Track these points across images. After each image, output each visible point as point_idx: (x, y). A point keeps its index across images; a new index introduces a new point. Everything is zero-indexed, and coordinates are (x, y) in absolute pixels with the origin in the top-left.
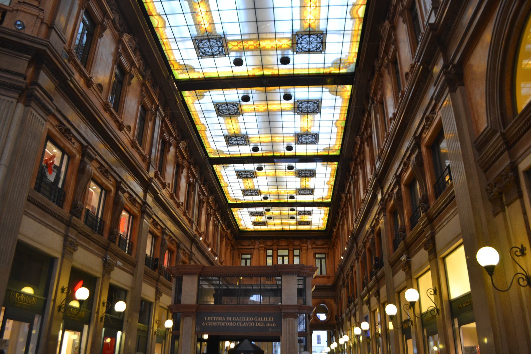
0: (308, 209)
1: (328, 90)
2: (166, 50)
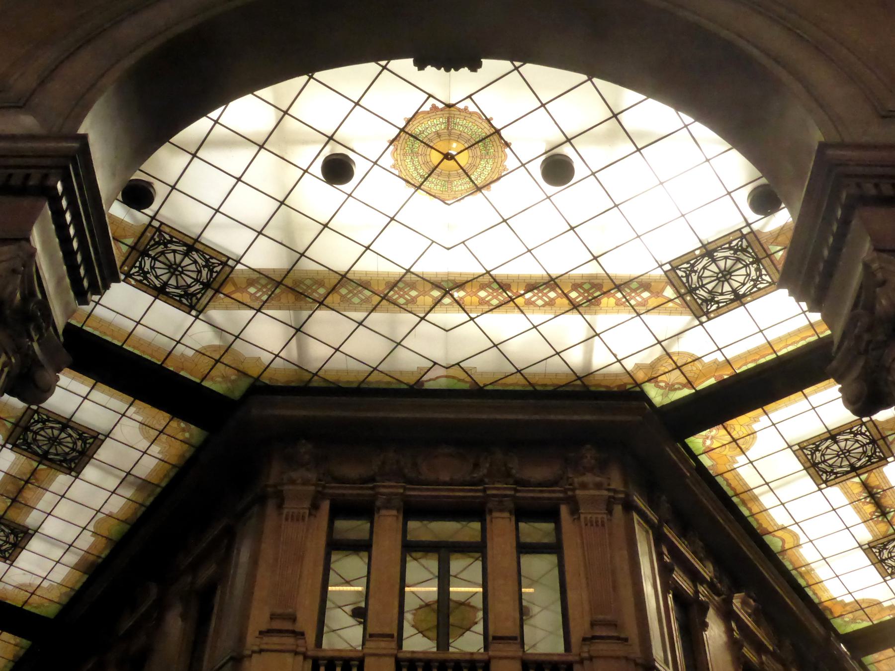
2: (809, 586)
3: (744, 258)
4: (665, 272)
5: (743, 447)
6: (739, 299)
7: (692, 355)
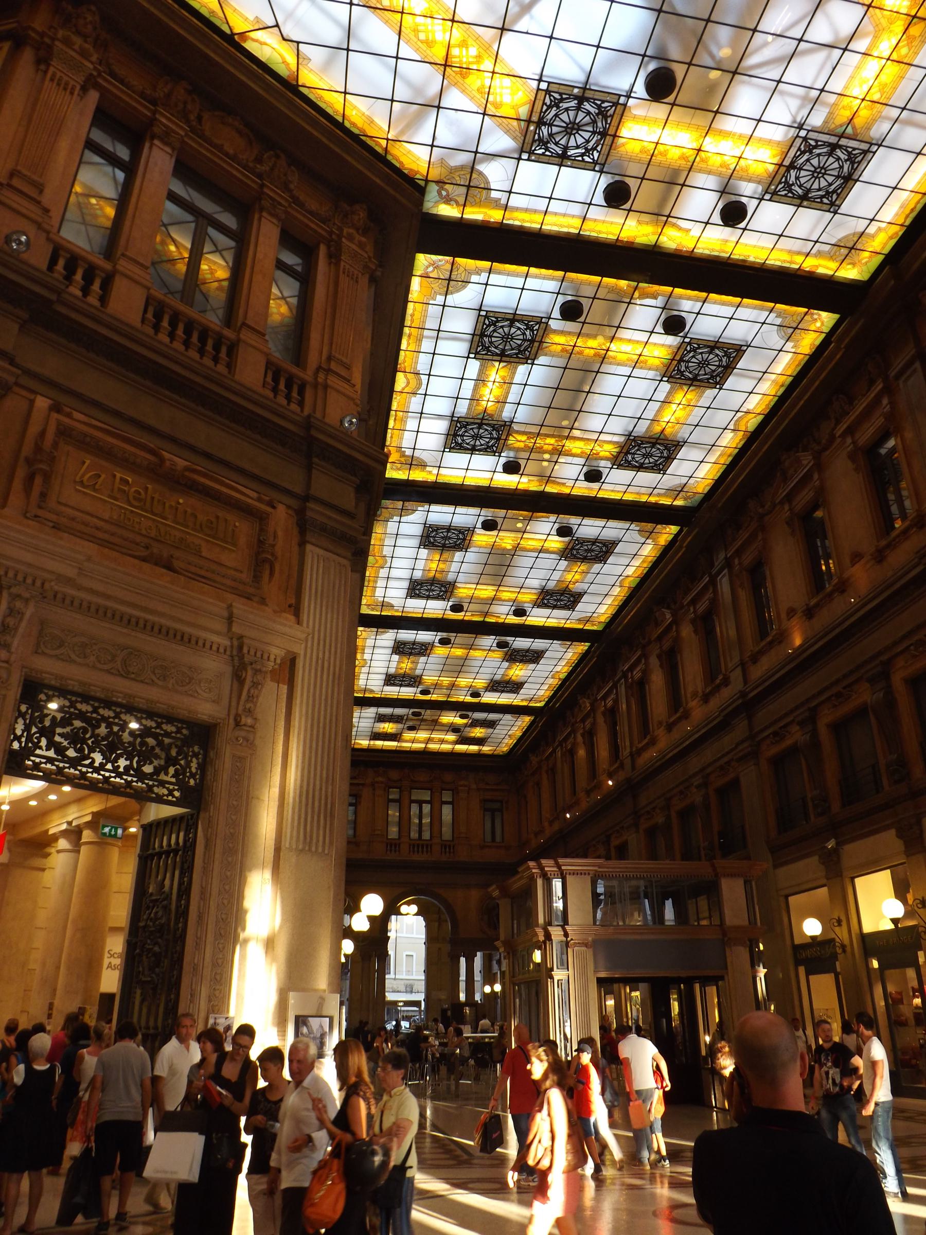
0: (492, 716)
1: (638, 528)
3: (600, 124)
4: (538, 89)
5: (450, 288)
6: (562, 159)
7: (488, 182)
